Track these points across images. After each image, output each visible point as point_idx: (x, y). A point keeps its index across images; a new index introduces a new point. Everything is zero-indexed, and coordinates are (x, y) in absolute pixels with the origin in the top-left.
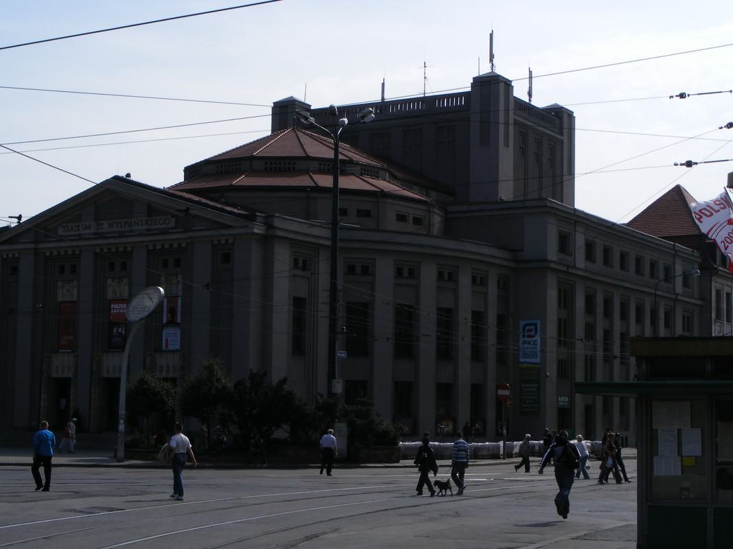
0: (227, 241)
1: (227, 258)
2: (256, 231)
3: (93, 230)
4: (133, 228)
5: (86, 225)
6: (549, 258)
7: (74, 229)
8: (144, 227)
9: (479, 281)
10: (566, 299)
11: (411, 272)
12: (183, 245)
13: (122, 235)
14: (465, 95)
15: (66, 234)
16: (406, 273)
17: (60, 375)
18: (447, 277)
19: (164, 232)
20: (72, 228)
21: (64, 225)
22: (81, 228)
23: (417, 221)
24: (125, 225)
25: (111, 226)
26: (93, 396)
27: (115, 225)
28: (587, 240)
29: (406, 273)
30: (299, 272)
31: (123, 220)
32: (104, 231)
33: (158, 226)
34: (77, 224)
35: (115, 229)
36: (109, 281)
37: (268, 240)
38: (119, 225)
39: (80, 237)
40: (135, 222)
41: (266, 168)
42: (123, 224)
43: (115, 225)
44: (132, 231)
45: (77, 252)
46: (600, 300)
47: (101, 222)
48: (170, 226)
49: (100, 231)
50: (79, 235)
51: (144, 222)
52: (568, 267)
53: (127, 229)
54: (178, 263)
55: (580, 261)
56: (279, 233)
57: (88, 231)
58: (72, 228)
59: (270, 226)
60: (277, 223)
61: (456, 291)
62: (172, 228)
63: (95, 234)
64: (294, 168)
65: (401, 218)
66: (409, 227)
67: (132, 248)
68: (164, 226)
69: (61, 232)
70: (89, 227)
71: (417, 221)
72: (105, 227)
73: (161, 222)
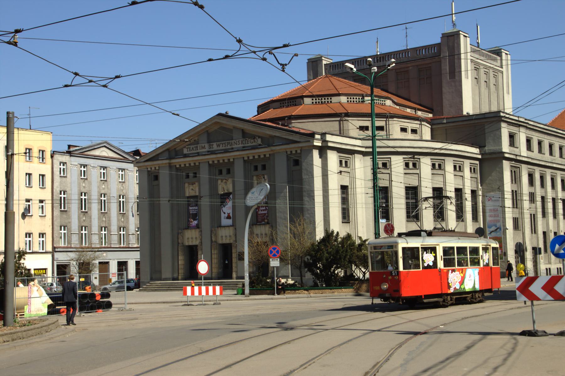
0: (296, 151)
1: (297, 163)
2: (315, 144)
4: (233, 147)
6: (504, 150)
8: (241, 145)
9: (458, 169)
10: (516, 178)
11: (414, 165)
12: (268, 156)
13: (226, 151)
14: (438, 45)
16: (411, 166)
17: (191, 244)
18: (437, 167)
19: (253, 148)
22: (199, 148)
23: (414, 131)
25: (218, 146)
26: (213, 256)
27: (221, 145)
28: (527, 137)
29: (411, 166)
30: (342, 169)
32: (213, 149)
34: (195, 146)
35: (221, 148)
36: (219, 182)
37: (323, 150)
39: (198, 154)
41: (313, 103)
43: (221, 145)
44: (232, 148)
45: (197, 164)
46: (537, 177)
49: (211, 149)
50: (198, 153)
52: (516, 155)
53: (229, 147)
54: (264, 167)
55: (523, 151)
56: (330, 144)
57: (204, 150)
59: (324, 141)
60: (329, 138)
61: (444, 176)
63: (208, 152)
64: (331, 102)
65: (404, 130)
66: (410, 135)
67: (234, 159)
69: (185, 151)
70: (204, 147)
71: (414, 131)
72: (215, 147)
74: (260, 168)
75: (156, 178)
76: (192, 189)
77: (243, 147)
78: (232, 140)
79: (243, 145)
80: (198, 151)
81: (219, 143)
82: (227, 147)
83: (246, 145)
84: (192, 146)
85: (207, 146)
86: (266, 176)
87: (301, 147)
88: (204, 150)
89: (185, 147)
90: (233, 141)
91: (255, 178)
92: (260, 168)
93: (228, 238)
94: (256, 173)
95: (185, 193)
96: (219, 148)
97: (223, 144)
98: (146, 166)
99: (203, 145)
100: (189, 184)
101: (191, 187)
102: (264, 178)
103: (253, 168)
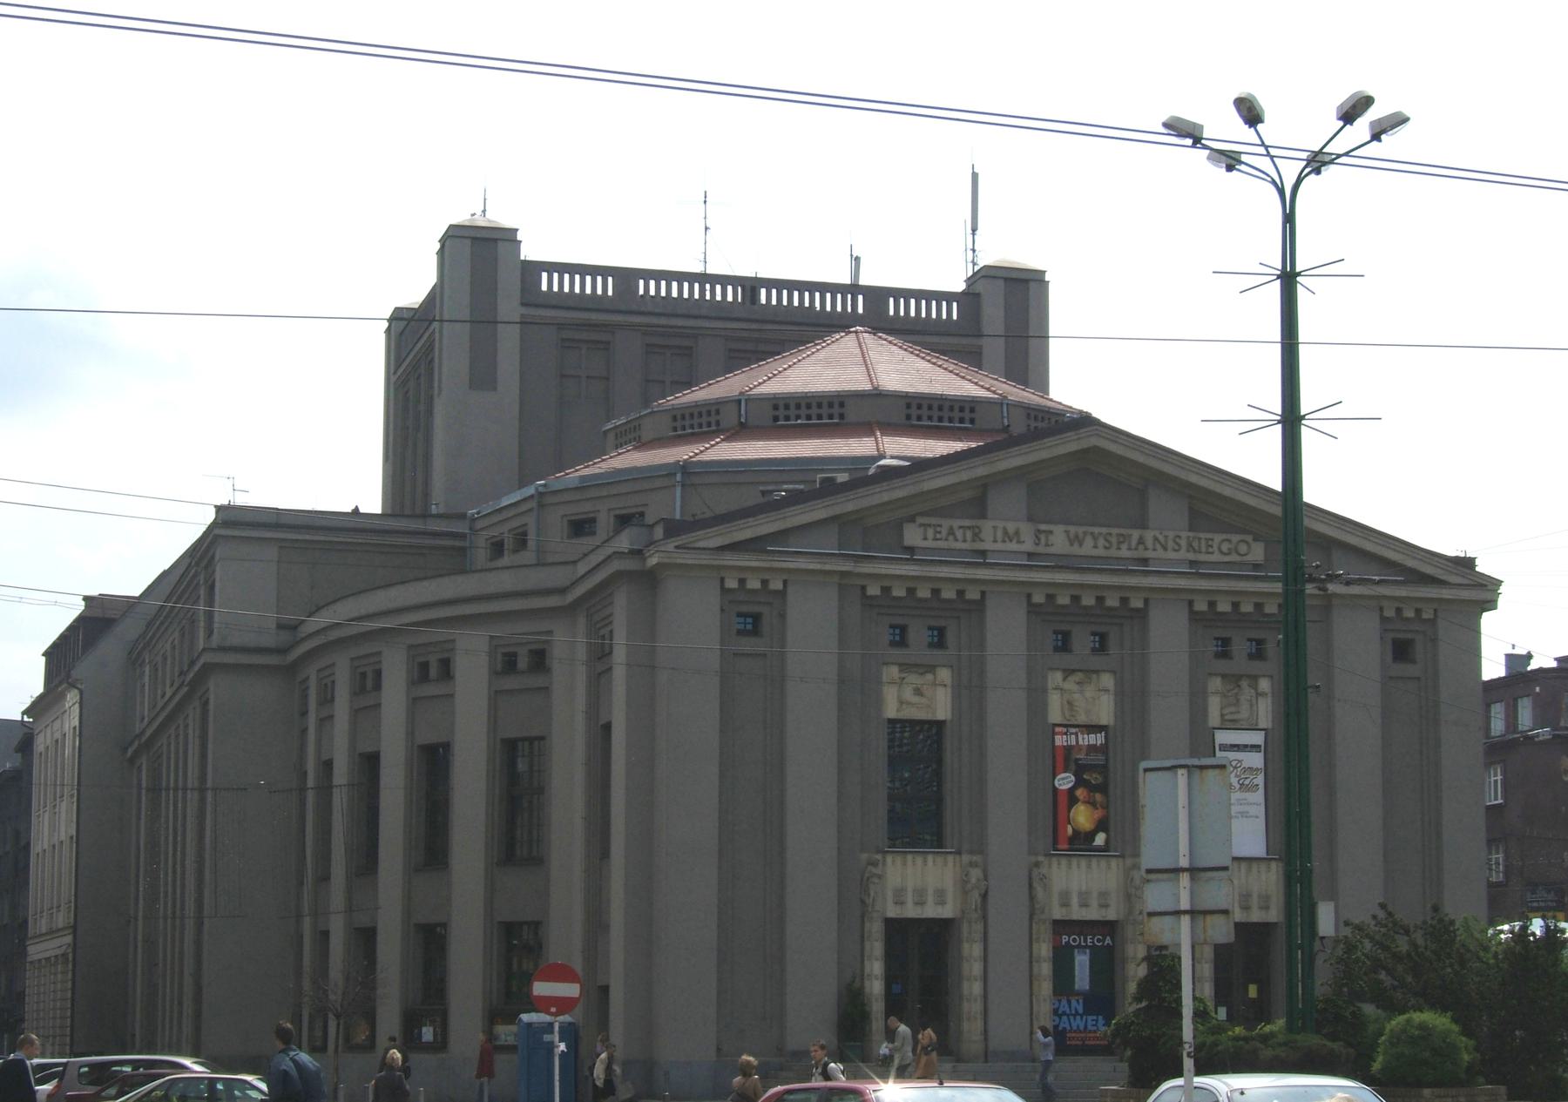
3: (1028, 546)
4: (1150, 554)
5: (1005, 532)
7: (959, 534)
8: (1184, 554)
15: (930, 544)
20: (951, 532)
21: (920, 520)
22: (987, 533)
24: (1119, 543)
27: (1089, 542)
31: (1115, 531)
33: (1216, 557)
35: (1087, 548)
38: (1101, 542)
40: (1156, 539)
42: (1114, 540)
43: (1089, 542)
44: (1145, 561)
47: (1043, 527)
48: (1249, 558)
49: (1041, 549)
51: (1183, 543)
57: (1013, 546)
58: (951, 532)
62: (1256, 567)
63: (1030, 555)
68: (1234, 558)
69: (912, 536)
70: (1007, 537)
72: (1059, 541)
73: (1225, 547)
74: (1240, 647)
75: (753, 625)
76: (918, 692)
77: (1192, 563)
78: (1144, 526)
79: (1191, 556)
80: (979, 546)
81: (1081, 530)
82: (1113, 552)
83: (1203, 557)
84: (946, 523)
85: (1027, 530)
86: (1264, 684)
87: (1440, 600)
88: (1013, 546)
89: (912, 519)
90: (1149, 536)
91: (1216, 684)
92: (1240, 647)
93: (1094, 903)
94: (1222, 665)
95: (879, 702)
96: (1076, 550)
97: (1095, 538)
98: (719, 568)
99: (1011, 527)
100: (905, 667)
101: (913, 679)
102: (1256, 689)
103: (1212, 648)
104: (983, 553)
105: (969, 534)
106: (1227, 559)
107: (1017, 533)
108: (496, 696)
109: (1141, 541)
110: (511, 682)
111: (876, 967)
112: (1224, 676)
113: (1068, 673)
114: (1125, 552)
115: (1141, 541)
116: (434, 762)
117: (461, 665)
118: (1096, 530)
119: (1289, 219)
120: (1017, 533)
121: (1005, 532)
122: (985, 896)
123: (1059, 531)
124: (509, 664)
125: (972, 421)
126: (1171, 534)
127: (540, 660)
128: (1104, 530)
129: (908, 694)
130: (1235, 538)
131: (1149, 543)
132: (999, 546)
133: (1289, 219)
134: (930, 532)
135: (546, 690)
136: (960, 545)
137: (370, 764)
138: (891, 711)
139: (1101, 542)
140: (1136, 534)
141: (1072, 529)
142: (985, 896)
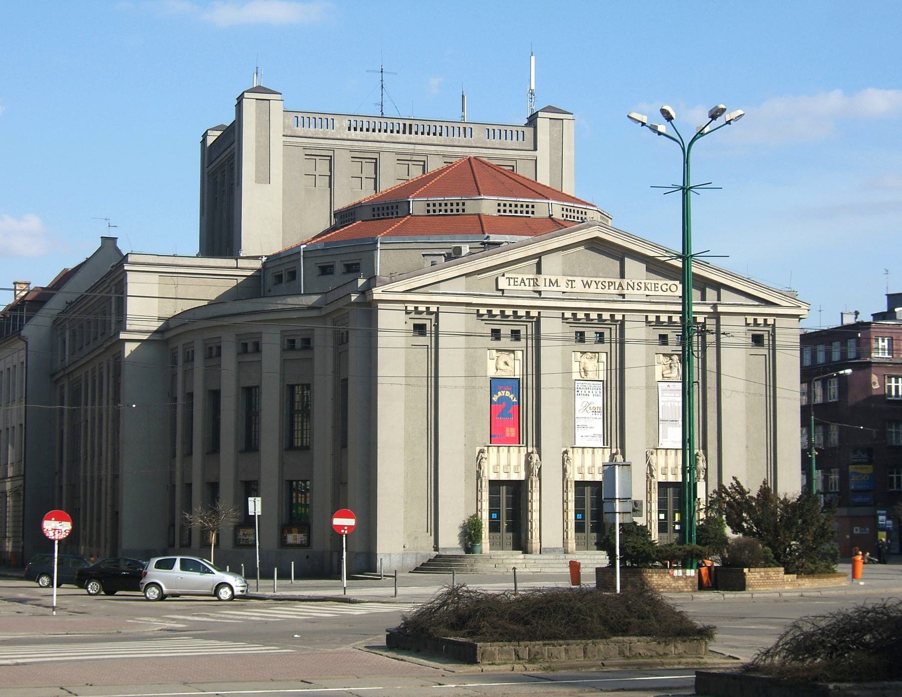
4: (625, 292)
5: (550, 281)
7: (527, 282)
15: (512, 287)
22: (541, 282)
25: (587, 284)
27: (594, 284)
31: (607, 280)
33: (660, 293)
35: (593, 288)
38: (600, 285)
42: (606, 284)
43: (594, 284)
51: (643, 286)
57: (555, 288)
68: (669, 293)
72: (578, 286)
73: (664, 288)
76: (506, 363)
80: (539, 289)
82: (606, 291)
84: (520, 277)
85: (562, 281)
89: (503, 275)
90: (625, 282)
100: (498, 350)
101: (504, 357)
104: (539, 292)
105: (532, 282)
106: (665, 294)
107: (557, 281)
108: (284, 362)
109: (620, 285)
110: (292, 355)
111: (486, 505)
112: (664, 355)
113: (583, 353)
114: (612, 291)
115: (620, 285)
116: (250, 396)
117: (265, 348)
118: (597, 280)
119: (686, 162)
120: (557, 281)
121: (550, 281)
122: (540, 469)
123: (578, 280)
124: (291, 345)
125: (533, 213)
126: (636, 282)
127: (307, 343)
128: (602, 280)
129: (501, 365)
130: (670, 282)
131: (625, 287)
132: (548, 288)
133: (686, 162)
134: (512, 281)
135: (311, 360)
136: (527, 288)
137: (215, 396)
138: (492, 373)
139: (600, 285)
140: (618, 281)
141: (585, 279)
142: (540, 469)
